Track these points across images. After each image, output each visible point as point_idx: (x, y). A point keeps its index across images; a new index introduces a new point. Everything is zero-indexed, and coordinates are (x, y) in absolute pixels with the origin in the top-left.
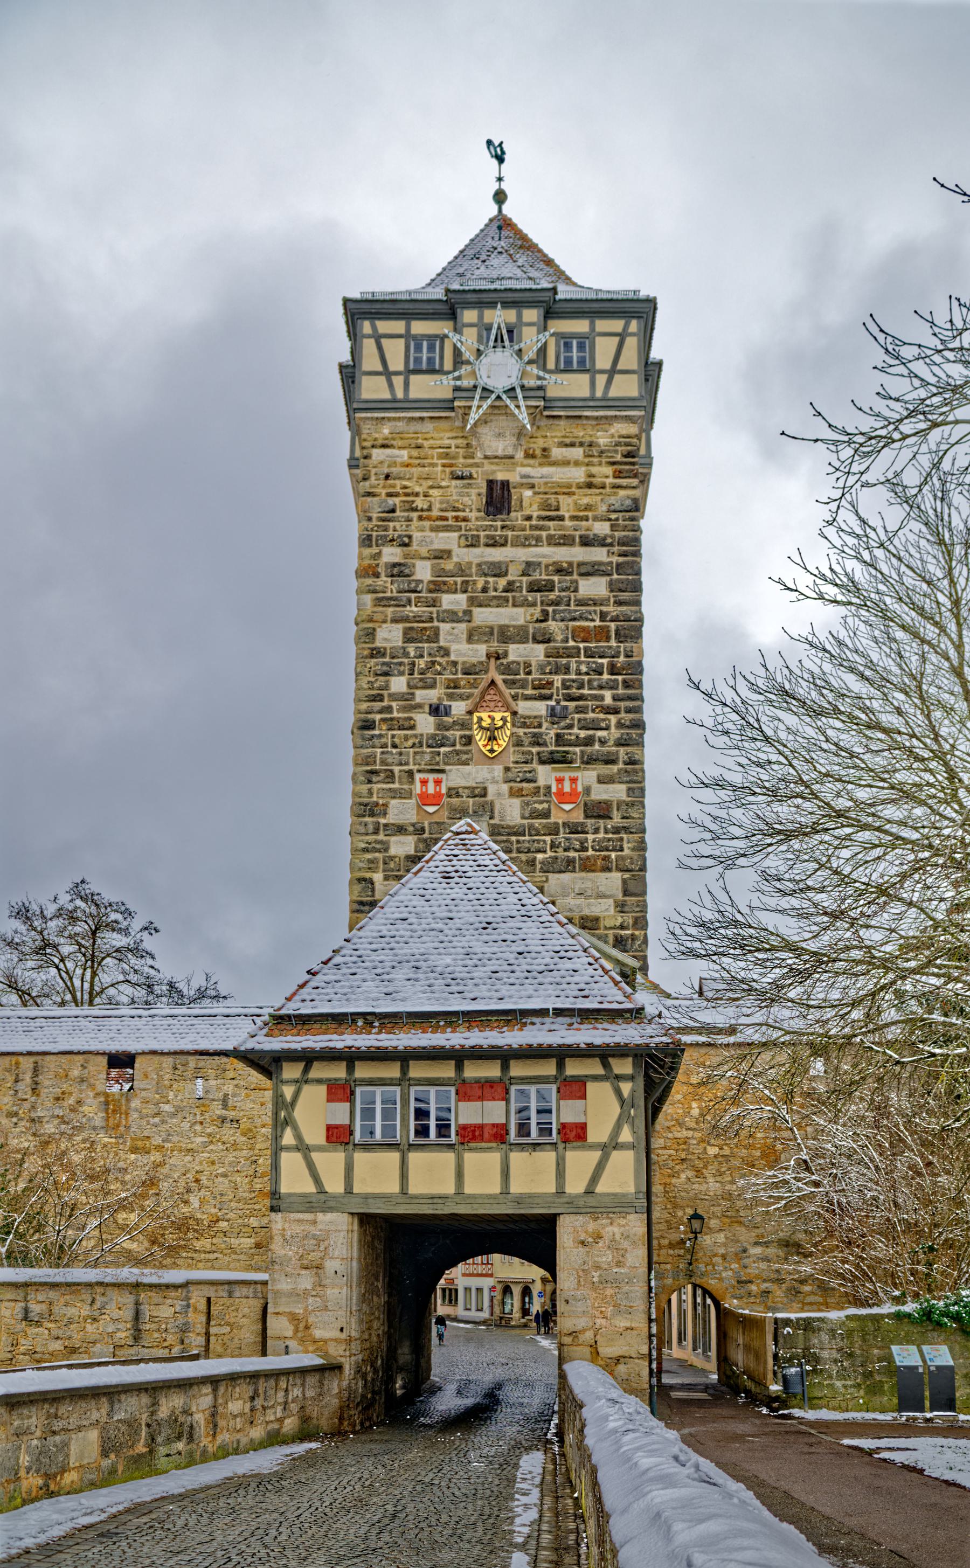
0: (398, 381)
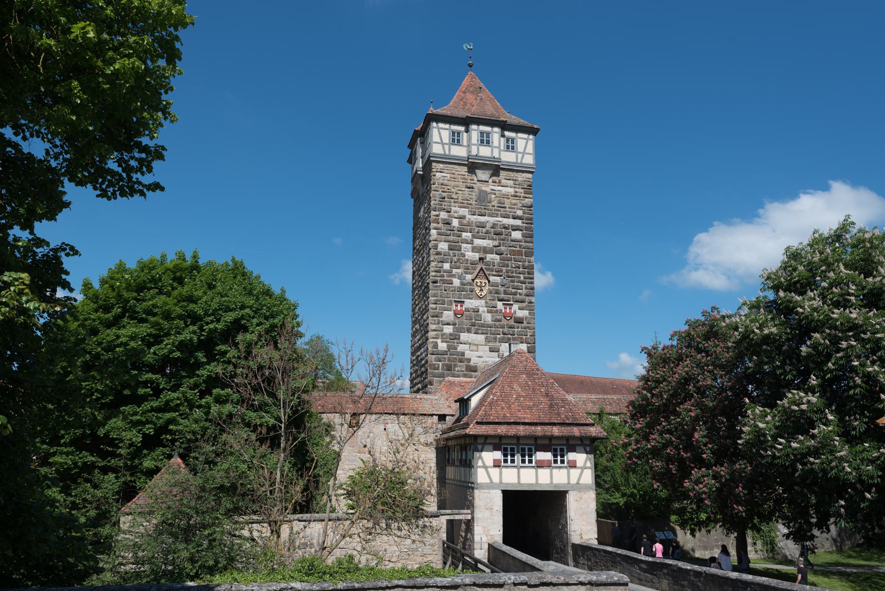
0: (446, 147)
